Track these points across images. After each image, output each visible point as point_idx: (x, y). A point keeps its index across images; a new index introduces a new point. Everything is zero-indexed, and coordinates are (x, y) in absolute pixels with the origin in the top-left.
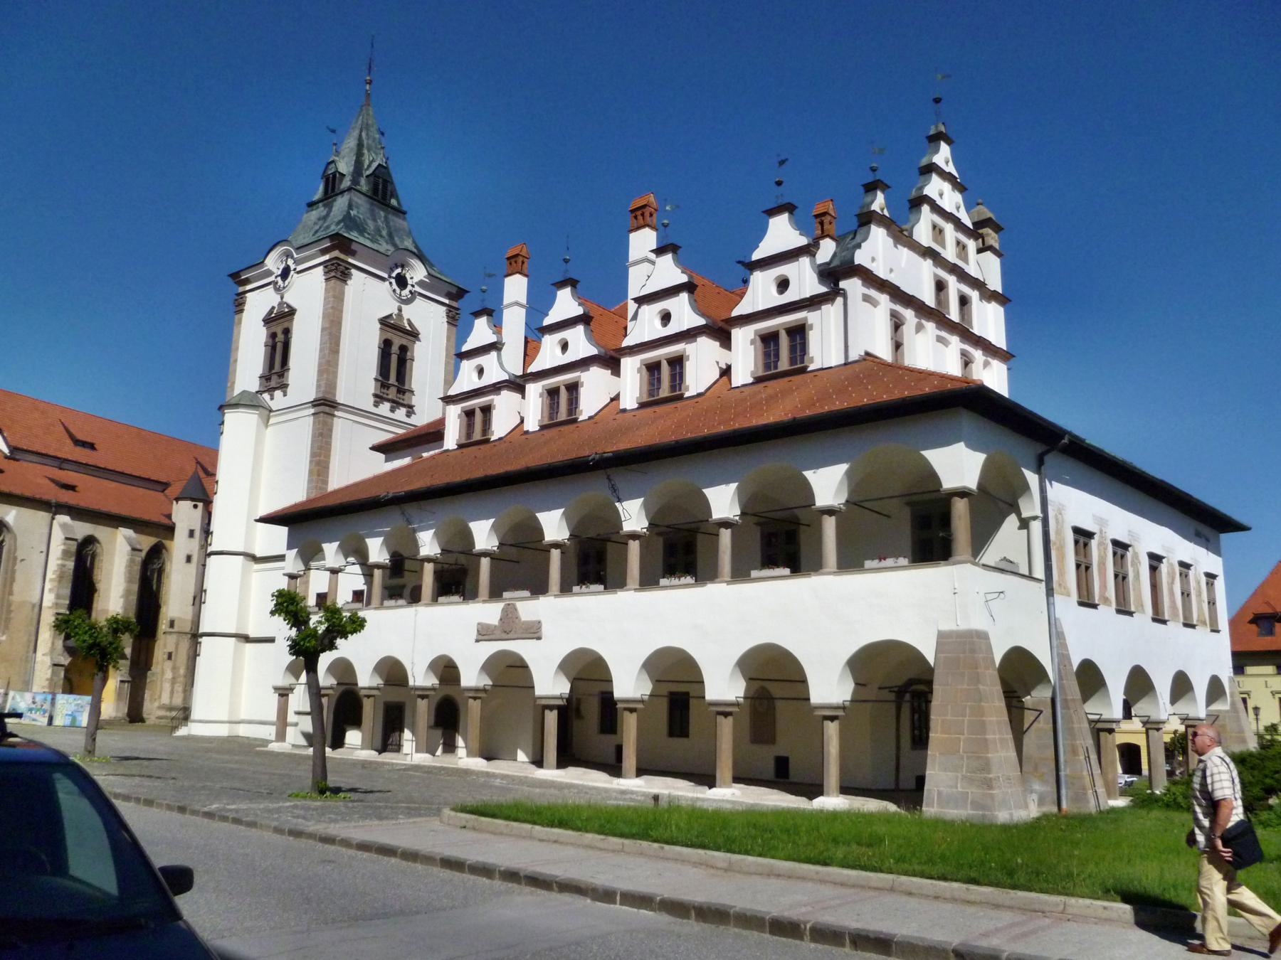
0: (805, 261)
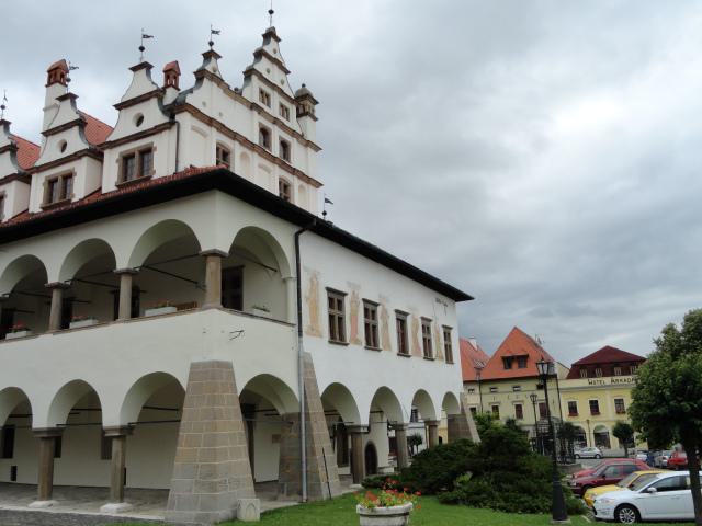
0: (154, 101)
